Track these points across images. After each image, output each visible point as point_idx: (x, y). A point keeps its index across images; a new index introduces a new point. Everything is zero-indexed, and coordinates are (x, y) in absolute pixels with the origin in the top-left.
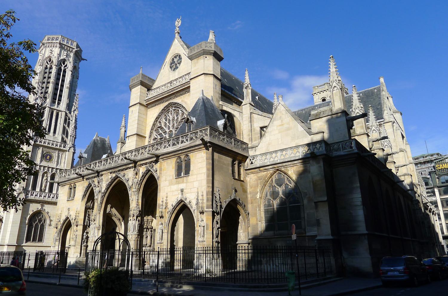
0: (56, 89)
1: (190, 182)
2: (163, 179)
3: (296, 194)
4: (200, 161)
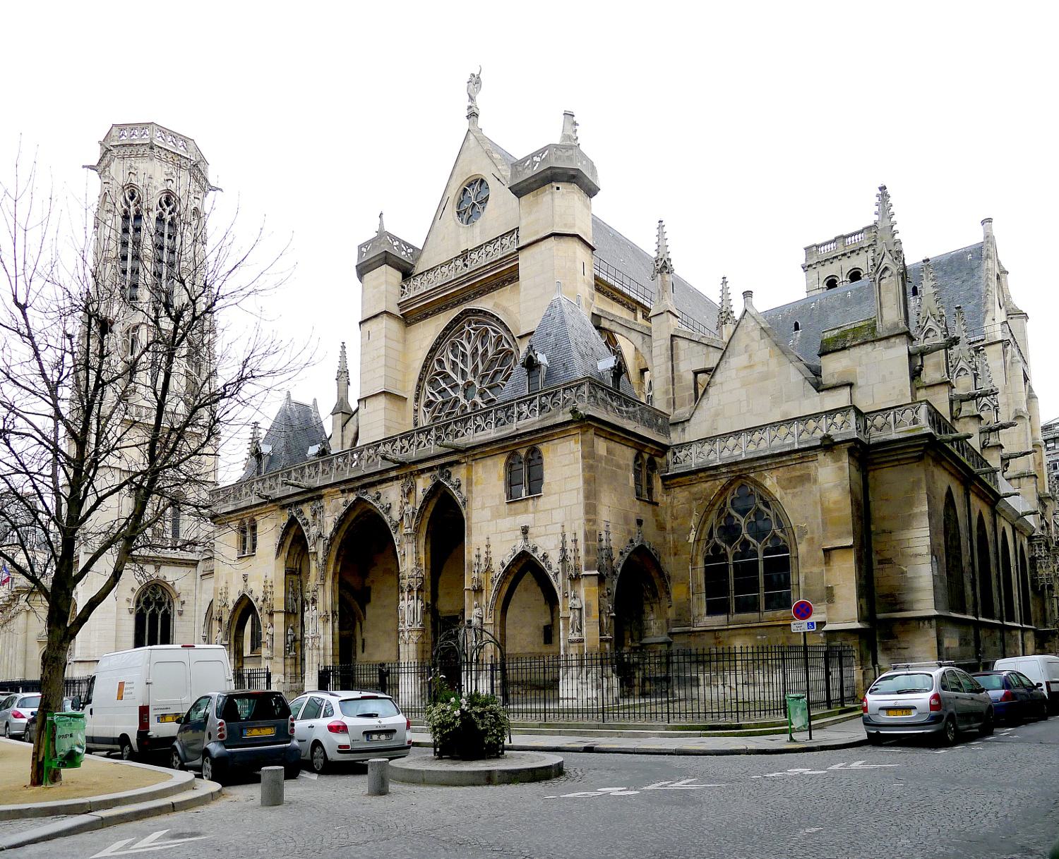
4: (567, 462)
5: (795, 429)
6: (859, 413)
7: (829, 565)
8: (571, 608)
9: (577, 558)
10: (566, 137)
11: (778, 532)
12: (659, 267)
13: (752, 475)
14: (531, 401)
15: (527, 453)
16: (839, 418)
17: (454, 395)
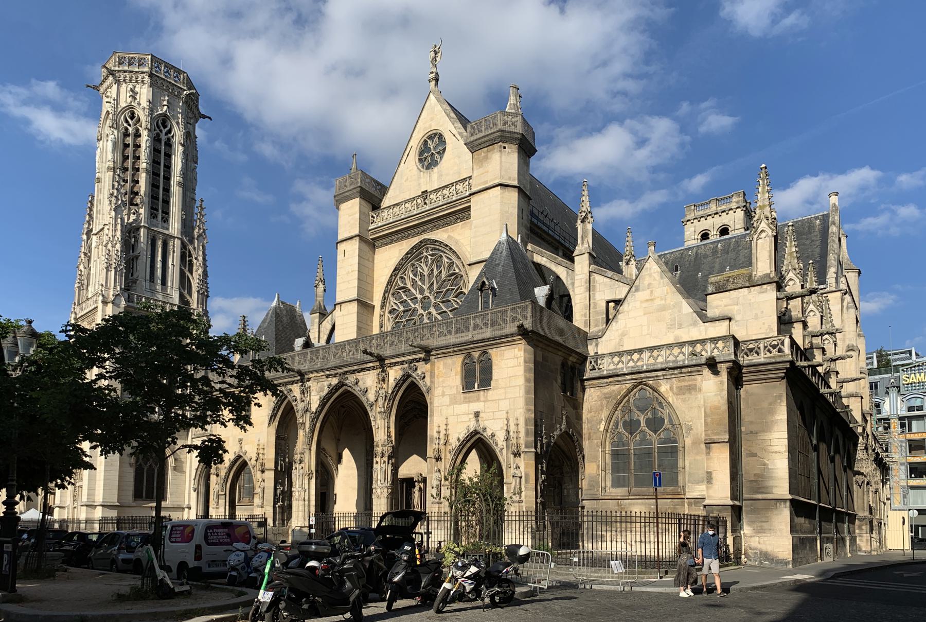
0: (153, 185)
1: (493, 401)
2: (438, 391)
7: (709, 455)
8: (513, 476)
13: (651, 382)
15: (480, 356)
17: (413, 306)
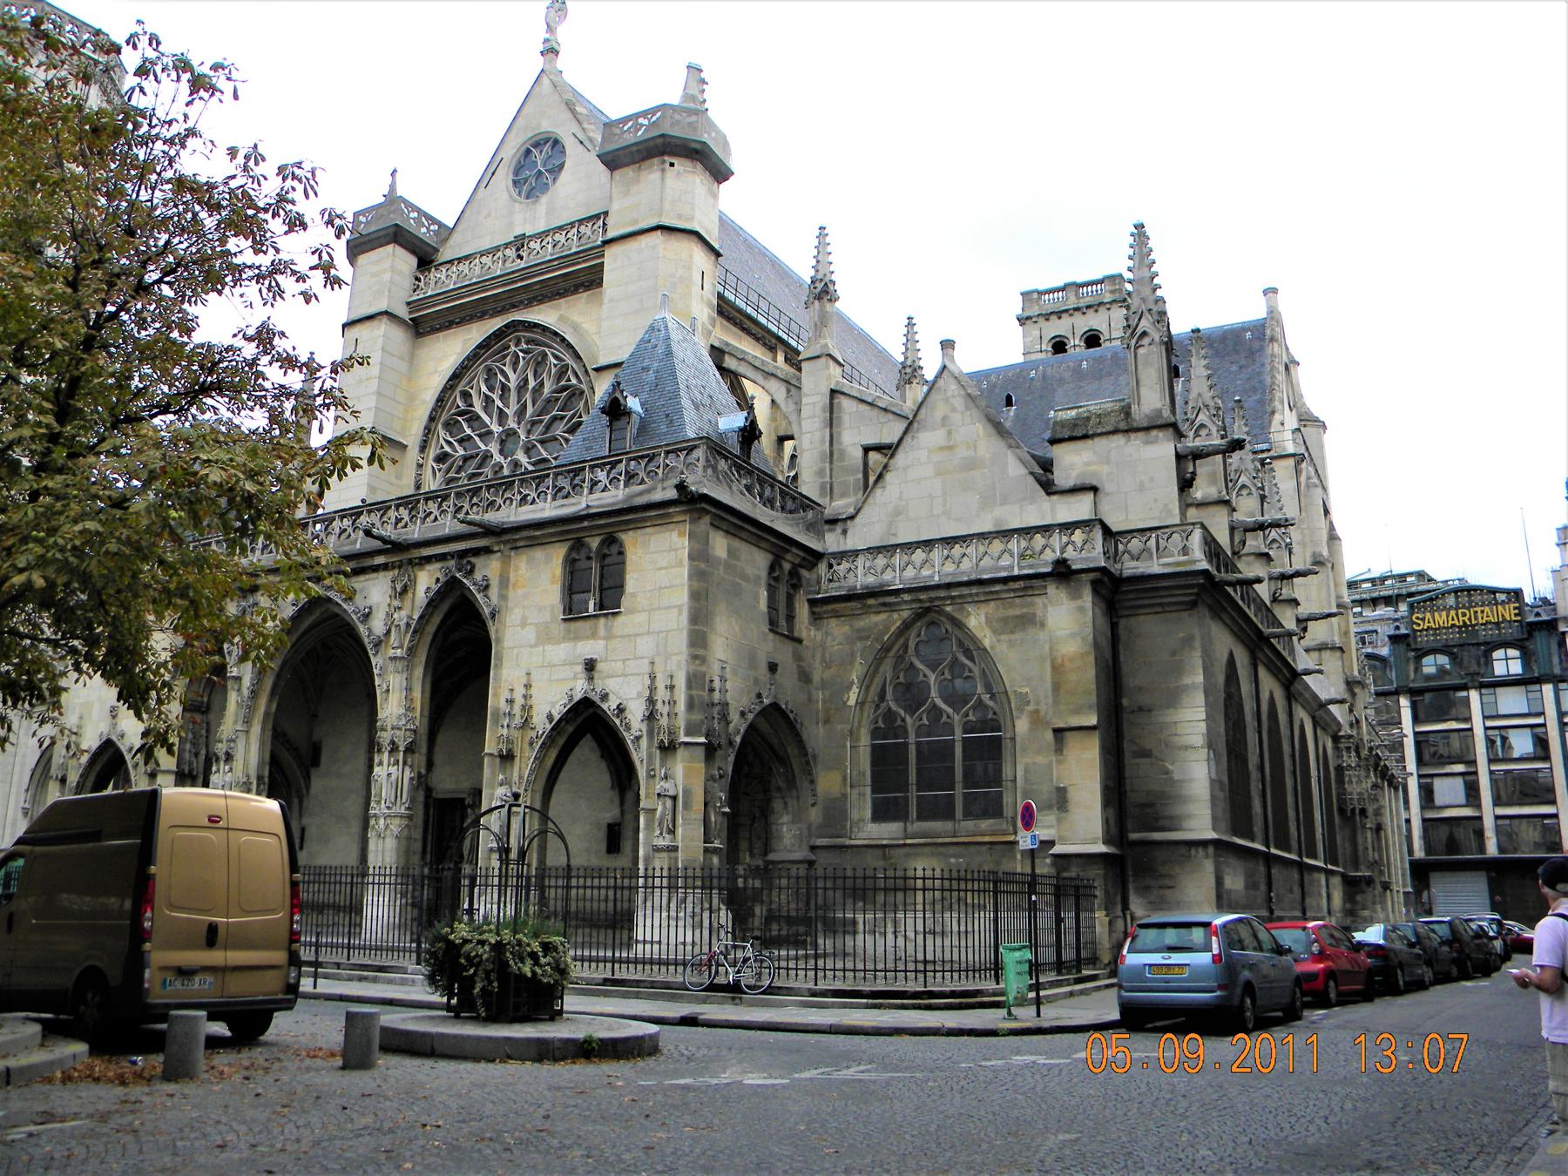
3: (991, 698)
4: (664, 564)
5: (1015, 545)
6: (1107, 532)
7: (1062, 754)
8: (659, 795)
9: (672, 715)
10: (687, 97)
11: (986, 697)
12: (817, 291)
13: (948, 609)
14: (614, 465)
15: (602, 543)
16: (1078, 536)
17: (483, 447)
